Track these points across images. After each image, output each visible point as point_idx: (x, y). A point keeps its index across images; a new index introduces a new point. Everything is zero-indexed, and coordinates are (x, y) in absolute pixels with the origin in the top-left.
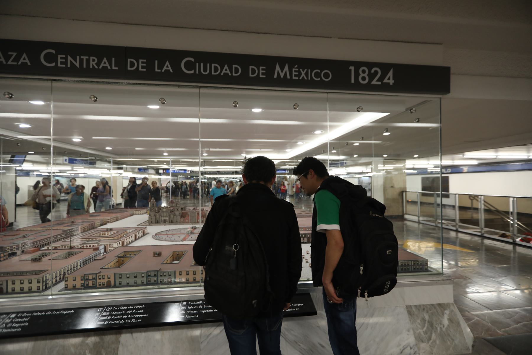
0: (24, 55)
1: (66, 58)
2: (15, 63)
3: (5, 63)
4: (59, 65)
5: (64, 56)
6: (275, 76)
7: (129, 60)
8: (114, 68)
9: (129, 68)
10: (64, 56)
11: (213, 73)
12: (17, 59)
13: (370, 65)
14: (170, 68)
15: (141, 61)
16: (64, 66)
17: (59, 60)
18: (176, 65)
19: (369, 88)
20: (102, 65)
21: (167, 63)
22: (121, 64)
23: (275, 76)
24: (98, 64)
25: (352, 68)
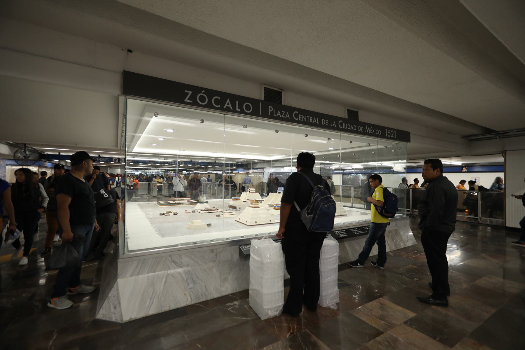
12: (285, 115)
13: (391, 129)
24: (313, 120)
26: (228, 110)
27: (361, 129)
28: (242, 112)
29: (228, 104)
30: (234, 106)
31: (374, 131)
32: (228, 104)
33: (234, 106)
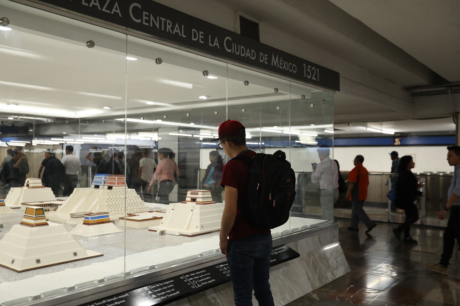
0: (116, 5)
1: (149, 16)
2: (109, 12)
3: (100, 9)
4: (144, 23)
5: (148, 14)
6: (272, 65)
7: (193, 30)
8: (184, 36)
9: (193, 39)
10: (148, 14)
11: (242, 55)
12: (110, 7)
14: (118, 11)
15: (201, 32)
16: (147, 24)
17: (144, 18)
20: (175, 30)
21: (216, 39)
23: (272, 65)
24: (173, 29)
25: (304, 65)
27: (264, 59)
31: (286, 66)
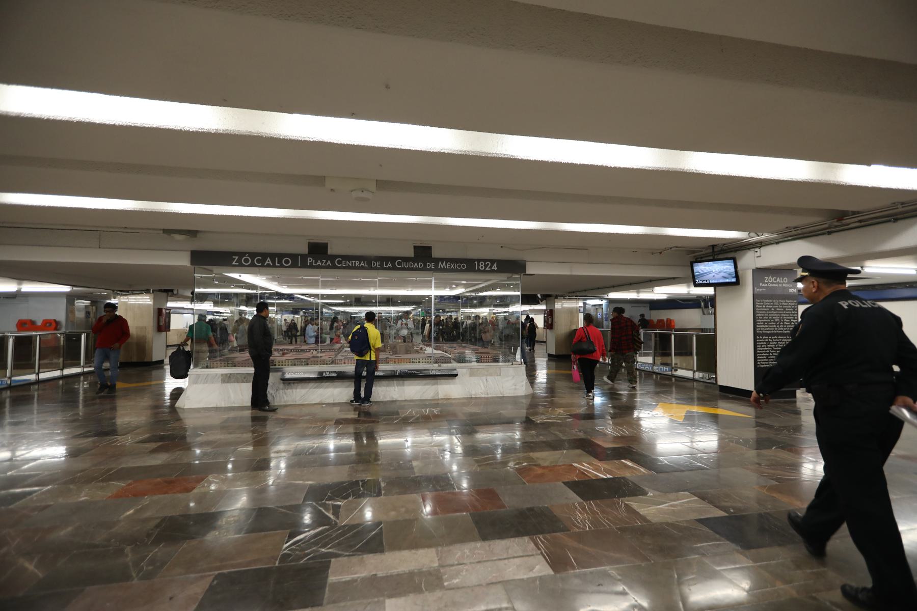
13: (485, 261)
18: (393, 264)
19: (485, 271)
22: (369, 264)
26: (268, 266)
27: (432, 265)
28: (282, 266)
29: (268, 261)
30: (274, 262)
32: (268, 261)
33: (274, 262)
